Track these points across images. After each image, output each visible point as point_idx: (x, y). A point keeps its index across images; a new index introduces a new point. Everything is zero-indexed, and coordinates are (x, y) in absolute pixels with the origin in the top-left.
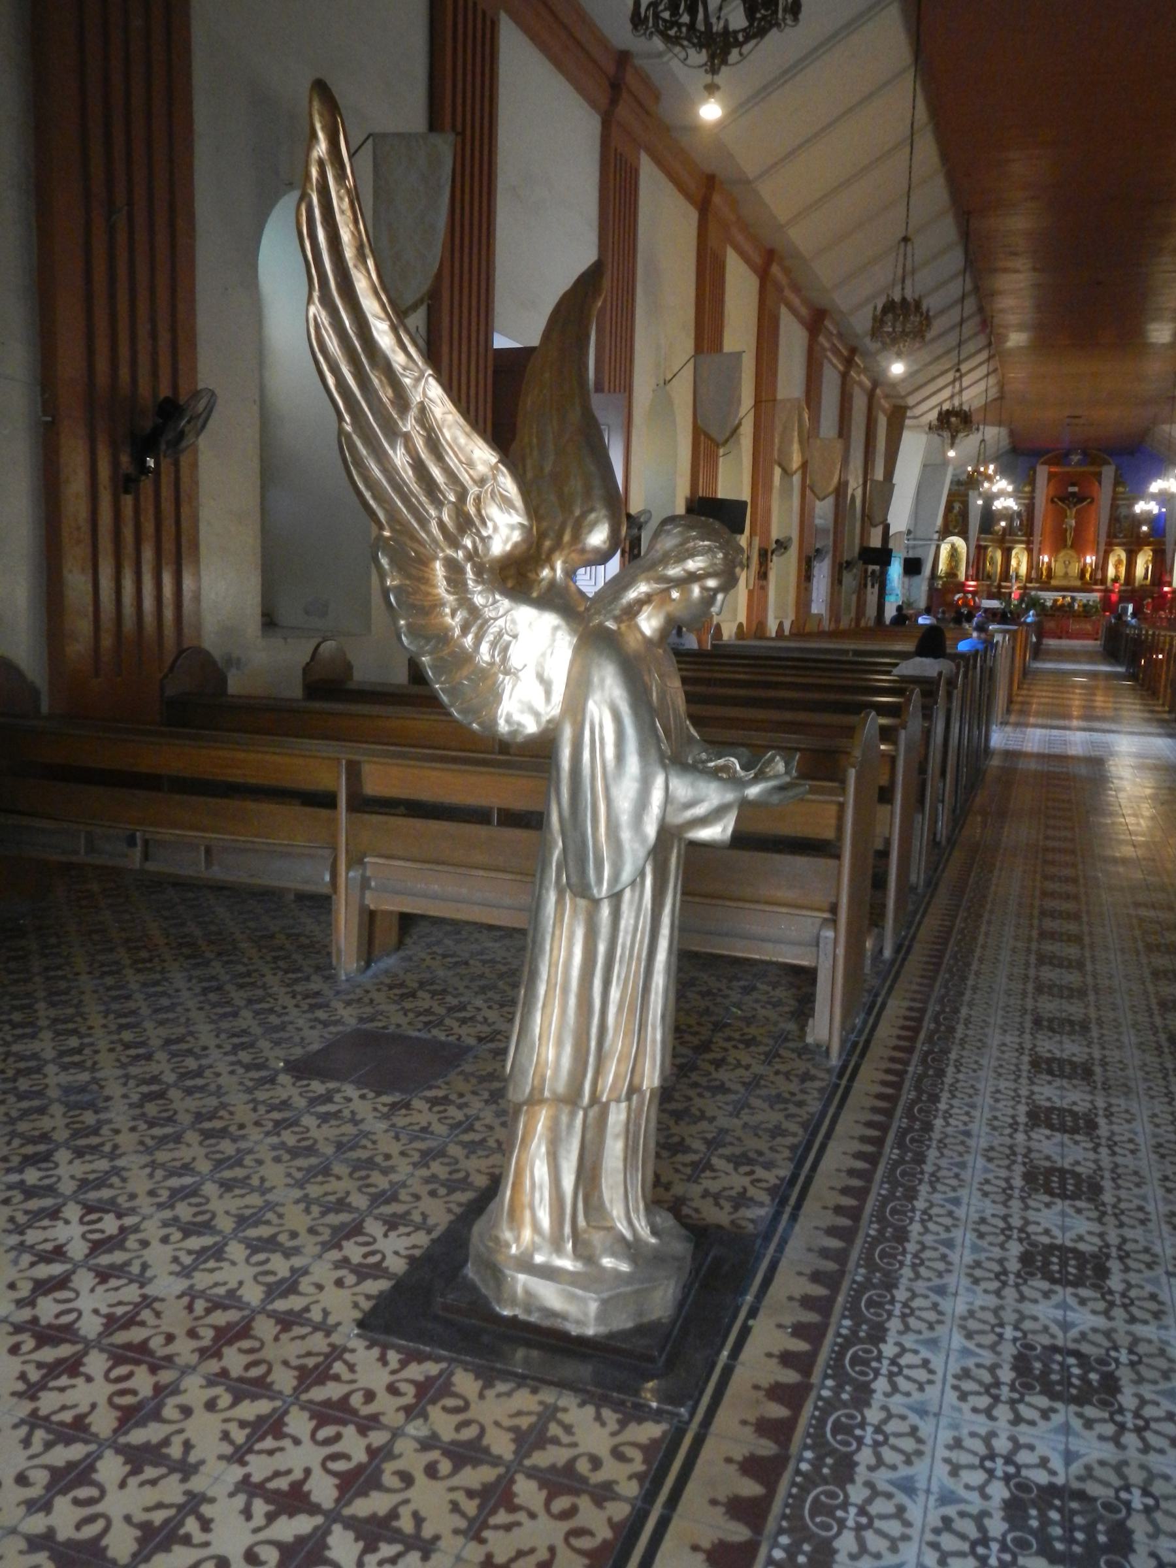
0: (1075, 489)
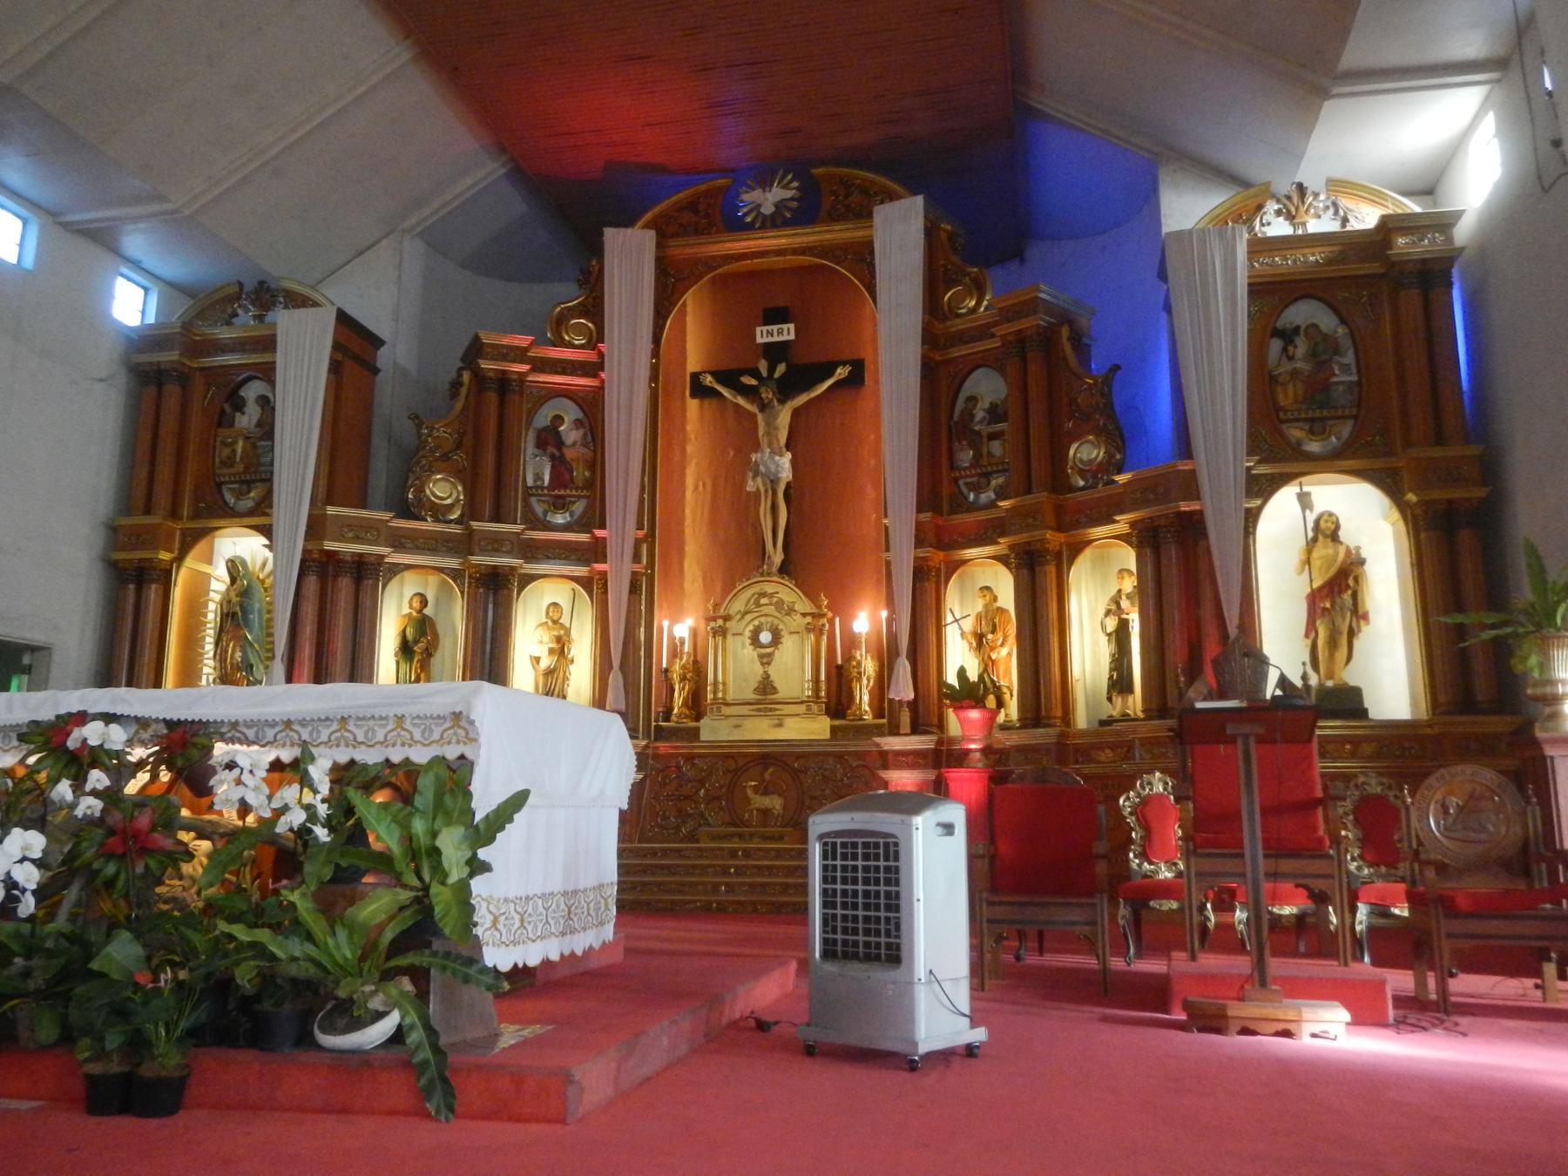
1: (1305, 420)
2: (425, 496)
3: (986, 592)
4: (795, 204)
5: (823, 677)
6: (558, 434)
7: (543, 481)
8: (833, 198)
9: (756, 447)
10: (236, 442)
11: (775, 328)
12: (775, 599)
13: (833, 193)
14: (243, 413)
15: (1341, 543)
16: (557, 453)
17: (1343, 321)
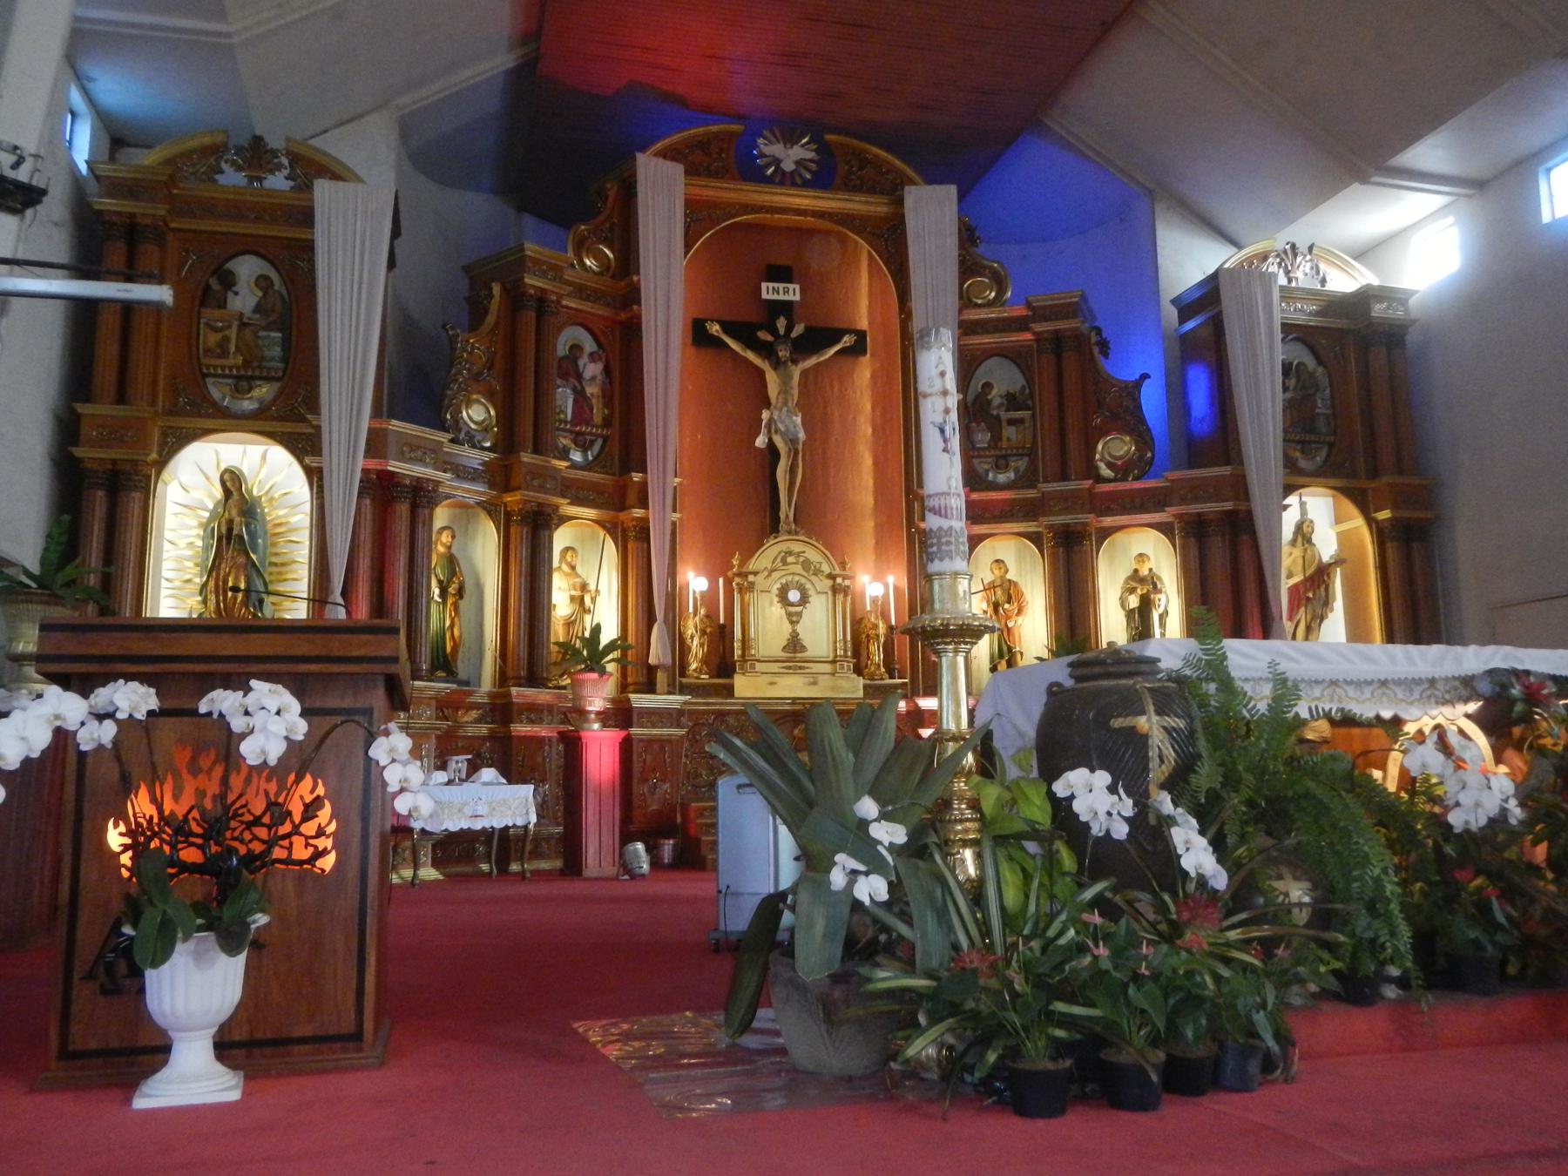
0: (791, 293)
1: (1299, 442)
2: (462, 417)
3: (1002, 565)
4: (813, 166)
5: (849, 638)
6: (577, 366)
7: (566, 415)
8: (846, 168)
9: (767, 404)
10: (229, 327)
11: (781, 286)
12: (802, 559)
13: (848, 163)
14: (236, 294)
15: (1314, 545)
16: (579, 388)
17: (1320, 362)
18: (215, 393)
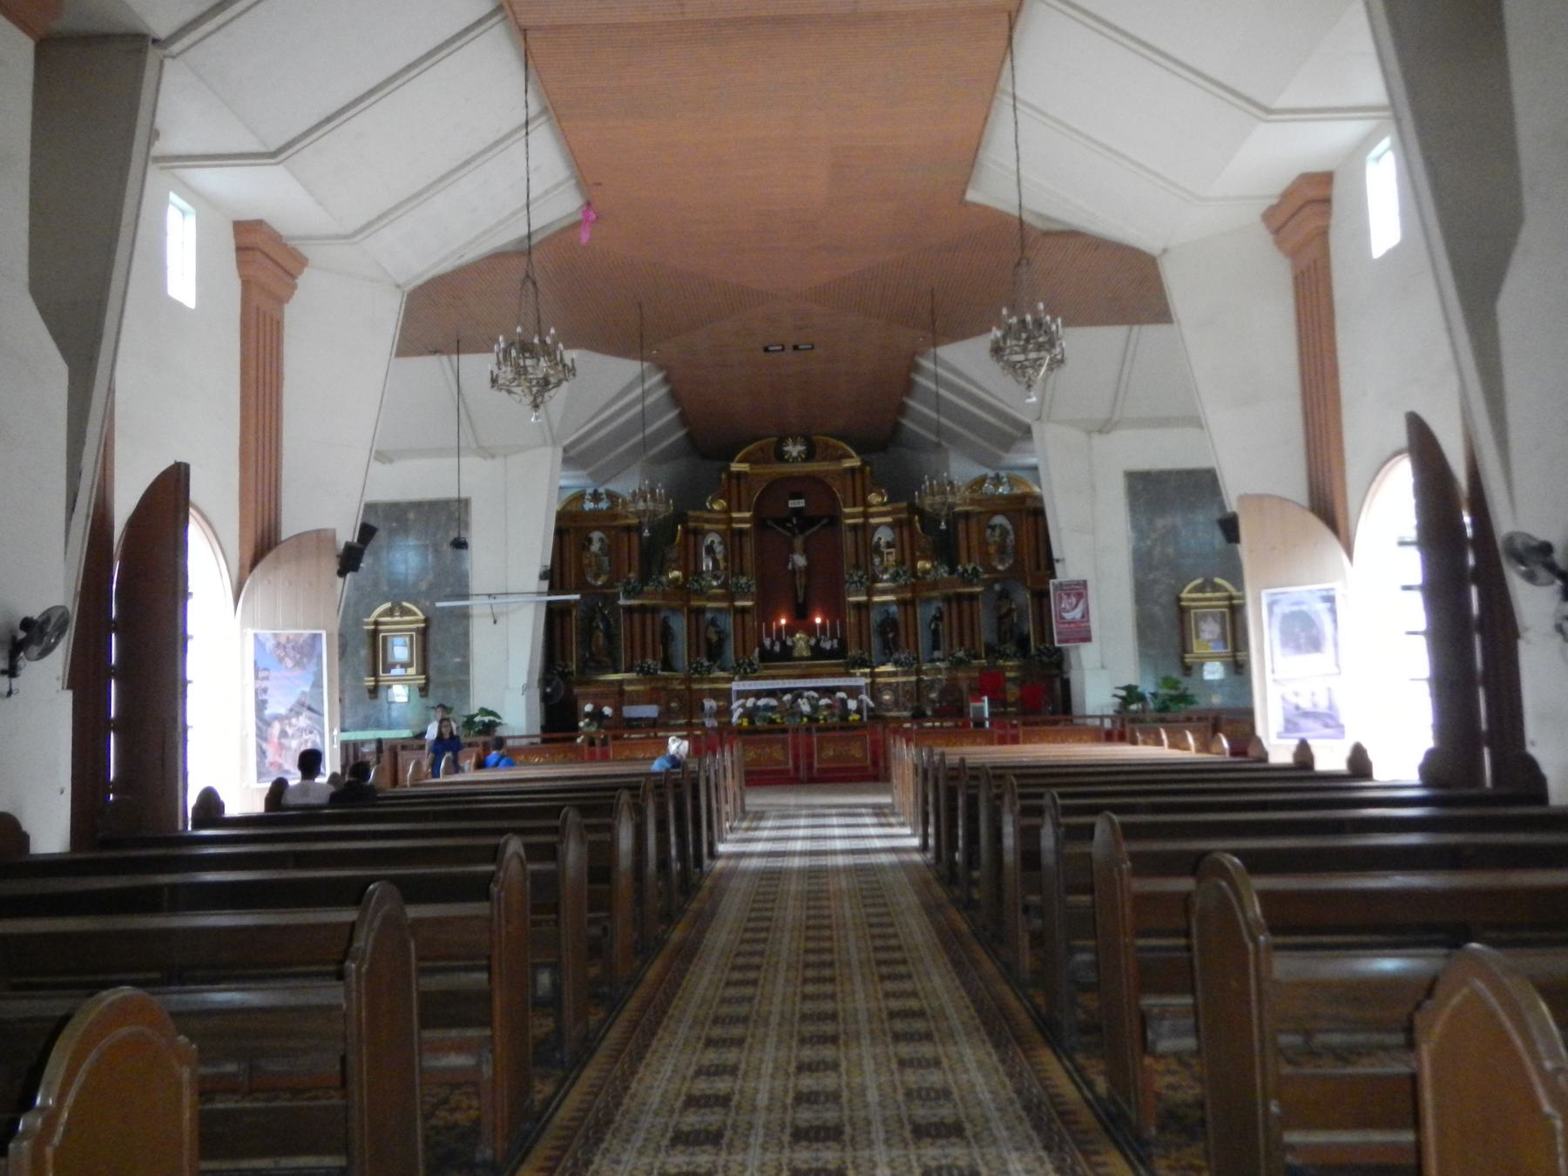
0: (801, 503)
18: (589, 579)
